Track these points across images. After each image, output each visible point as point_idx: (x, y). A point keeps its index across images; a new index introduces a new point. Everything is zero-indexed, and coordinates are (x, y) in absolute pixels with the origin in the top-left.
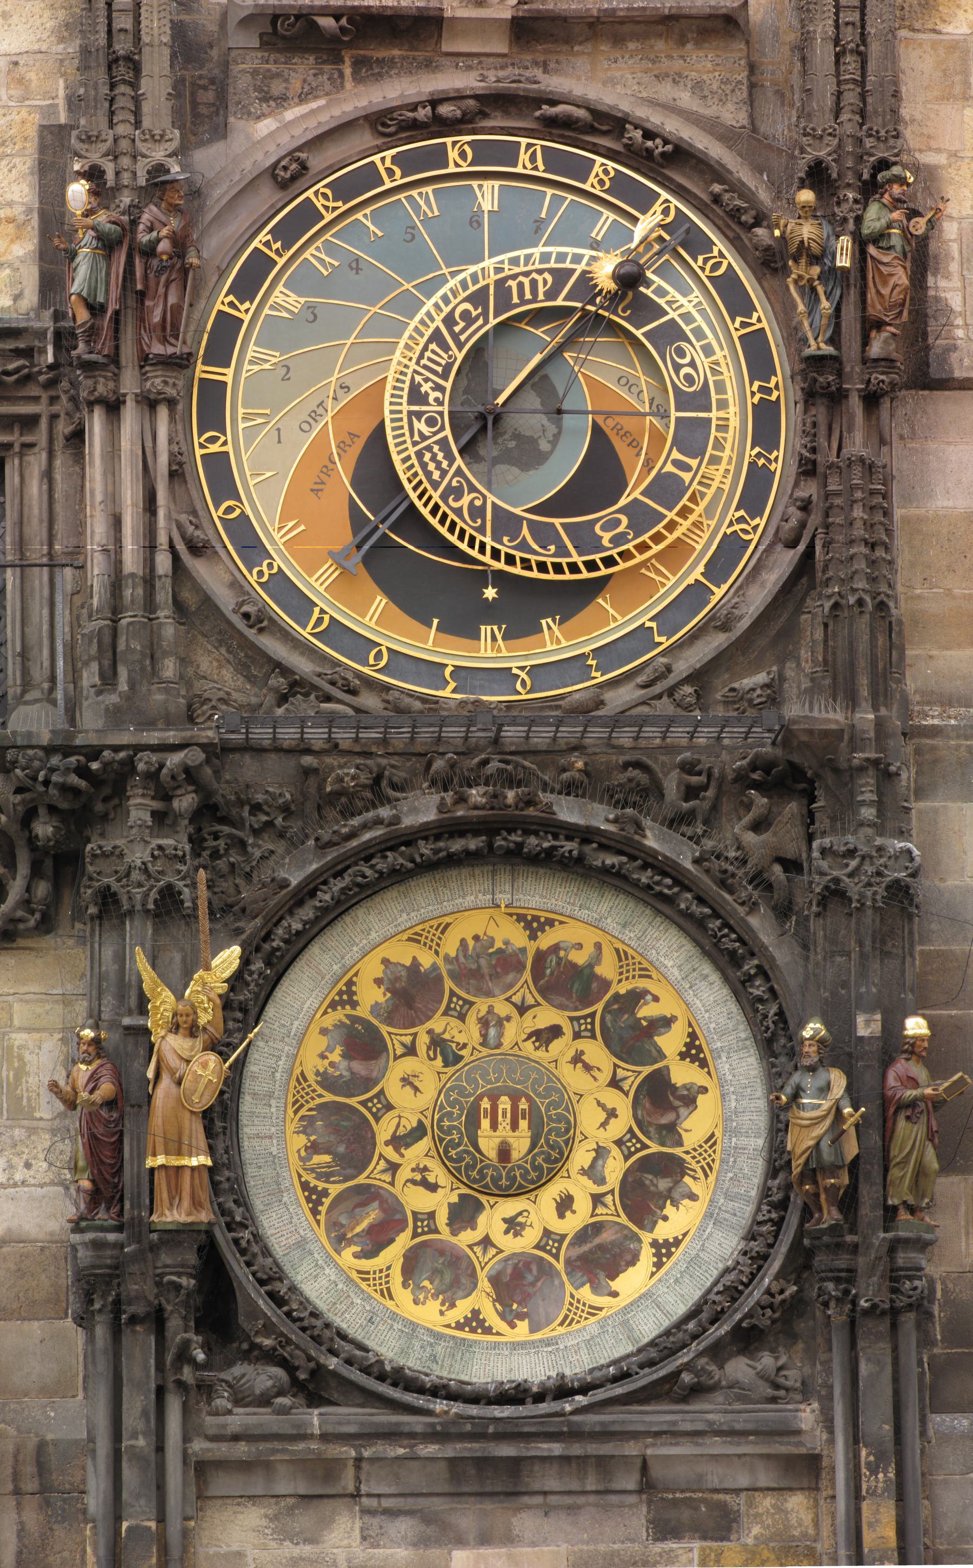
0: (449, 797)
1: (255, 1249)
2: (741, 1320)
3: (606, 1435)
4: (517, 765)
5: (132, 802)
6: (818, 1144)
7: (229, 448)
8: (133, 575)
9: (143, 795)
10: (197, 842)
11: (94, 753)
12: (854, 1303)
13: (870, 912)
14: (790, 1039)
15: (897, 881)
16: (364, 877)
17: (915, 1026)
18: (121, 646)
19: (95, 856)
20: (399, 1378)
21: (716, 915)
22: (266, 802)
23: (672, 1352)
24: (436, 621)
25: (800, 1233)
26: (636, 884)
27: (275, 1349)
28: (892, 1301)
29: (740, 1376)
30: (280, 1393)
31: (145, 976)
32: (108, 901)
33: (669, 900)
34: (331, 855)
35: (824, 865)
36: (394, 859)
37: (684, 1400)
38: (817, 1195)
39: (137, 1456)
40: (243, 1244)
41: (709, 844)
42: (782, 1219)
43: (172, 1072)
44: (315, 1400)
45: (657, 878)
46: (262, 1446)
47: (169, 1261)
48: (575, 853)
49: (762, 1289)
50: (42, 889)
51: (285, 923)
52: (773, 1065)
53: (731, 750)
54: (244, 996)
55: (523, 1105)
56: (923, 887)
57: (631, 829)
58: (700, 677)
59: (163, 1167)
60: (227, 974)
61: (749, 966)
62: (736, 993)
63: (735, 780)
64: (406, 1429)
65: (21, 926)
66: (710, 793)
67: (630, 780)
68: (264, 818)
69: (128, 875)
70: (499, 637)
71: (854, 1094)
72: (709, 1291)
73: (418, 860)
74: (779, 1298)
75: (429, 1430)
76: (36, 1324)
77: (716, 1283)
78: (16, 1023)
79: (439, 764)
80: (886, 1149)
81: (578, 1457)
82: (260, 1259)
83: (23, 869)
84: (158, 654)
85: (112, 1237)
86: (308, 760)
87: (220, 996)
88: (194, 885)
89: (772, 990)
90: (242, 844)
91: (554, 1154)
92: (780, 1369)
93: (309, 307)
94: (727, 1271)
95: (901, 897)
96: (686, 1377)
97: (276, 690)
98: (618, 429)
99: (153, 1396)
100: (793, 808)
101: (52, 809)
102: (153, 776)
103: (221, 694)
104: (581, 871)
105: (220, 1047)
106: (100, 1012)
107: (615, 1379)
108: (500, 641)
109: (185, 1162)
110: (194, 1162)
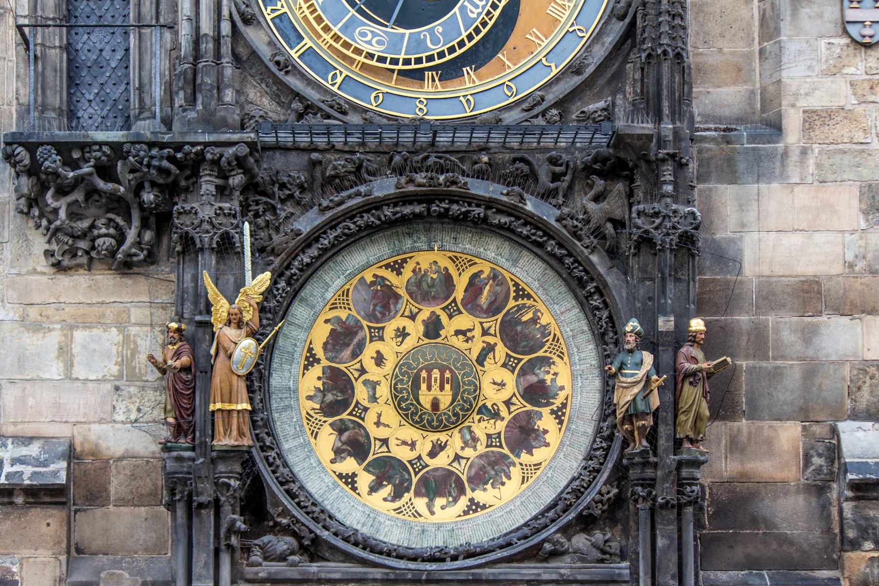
0: (403, 180)
1: (278, 462)
2: (582, 510)
4: (447, 159)
5: (203, 179)
10: (245, 208)
12: (654, 499)
14: (616, 333)
18: (199, 81)
19: (180, 213)
20: (366, 544)
21: (570, 255)
22: (289, 182)
23: (538, 531)
25: (621, 456)
26: (520, 235)
28: (678, 499)
29: (581, 545)
30: (293, 553)
31: (209, 290)
32: (188, 241)
33: (541, 245)
34: (329, 214)
35: (639, 222)
36: (370, 218)
37: (545, 560)
41: (566, 210)
42: (609, 447)
44: (314, 557)
45: (533, 231)
47: (223, 470)
48: (482, 215)
49: (596, 491)
50: (148, 236)
52: (605, 350)
53: (581, 150)
54: (273, 304)
55: (448, 375)
56: (702, 237)
57: (517, 199)
58: (562, 104)
59: (219, 410)
60: (263, 289)
61: (591, 287)
62: (581, 304)
63: (584, 169)
64: (371, 577)
65: (135, 259)
66: (568, 178)
67: (517, 169)
68: (288, 192)
69: (200, 226)
70: (437, 79)
73: (383, 219)
74: (606, 497)
75: (385, 577)
76: (143, 509)
78: (133, 320)
79: (397, 158)
80: (676, 403)
82: (281, 469)
83: (136, 223)
85: (187, 454)
86: (315, 156)
87: (257, 303)
88: (242, 233)
89: (605, 302)
90: (274, 208)
91: (467, 406)
92: (606, 542)
94: (574, 479)
95: (687, 243)
96: (548, 546)
97: (296, 111)
99: (212, 555)
100: (620, 186)
101: (153, 184)
103: (262, 113)
104: (485, 227)
106: (183, 313)
109: (233, 407)
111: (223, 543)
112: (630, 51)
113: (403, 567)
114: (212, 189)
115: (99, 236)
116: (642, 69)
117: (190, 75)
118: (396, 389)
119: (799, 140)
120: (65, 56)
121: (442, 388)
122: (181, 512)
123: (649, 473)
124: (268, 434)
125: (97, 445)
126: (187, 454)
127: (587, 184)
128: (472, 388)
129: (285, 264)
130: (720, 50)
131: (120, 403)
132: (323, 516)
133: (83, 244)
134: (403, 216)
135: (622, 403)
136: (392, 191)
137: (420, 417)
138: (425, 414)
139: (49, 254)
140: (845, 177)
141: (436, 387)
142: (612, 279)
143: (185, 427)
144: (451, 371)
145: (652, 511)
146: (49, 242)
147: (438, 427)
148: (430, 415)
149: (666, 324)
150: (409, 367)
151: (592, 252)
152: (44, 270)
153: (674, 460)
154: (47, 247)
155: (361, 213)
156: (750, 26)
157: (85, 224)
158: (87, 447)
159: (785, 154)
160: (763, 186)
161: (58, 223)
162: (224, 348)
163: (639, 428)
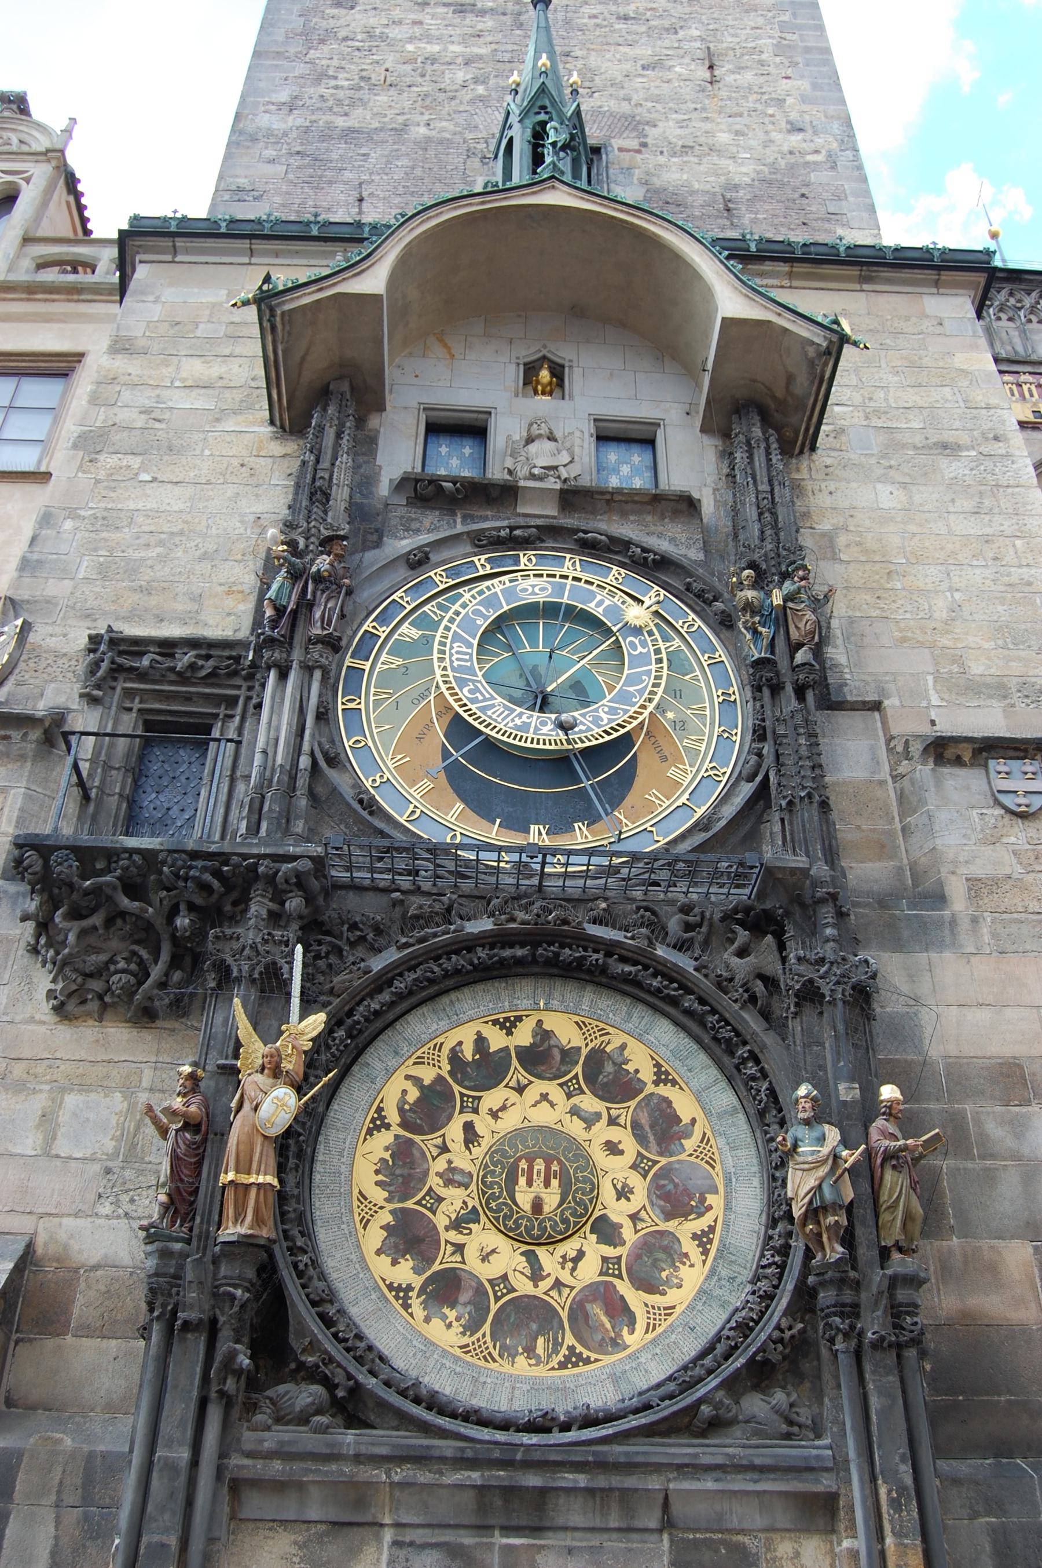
1: (311, 1271)
2: (755, 1354)
3: (630, 1467)
6: (820, 1186)
7: (362, 706)
9: (263, 896)
11: (223, 857)
13: (840, 1004)
14: (780, 1110)
16: (433, 972)
18: (266, 808)
19: (217, 937)
20: (433, 1403)
21: (714, 1011)
23: (688, 1386)
24: (498, 821)
30: (319, 1412)
37: (703, 1434)
39: (171, 1467)
40: (301, 1266)
42: (785, 1263)
44: (354, 1420)
46: (296, 1466)
47: (229, 1273)
48: (600, 961)
55: (555, 1167)
60: (315, 1033)
61: (742, 1051)
63: (723, 920)
64: (437, 1453)
66: (704, 929)
70: (544, 832)
71: (845, 1142)
72: (723, 1328)
74: (788, 1334)
75: (459, 1455)
76: (114, 1342)
77: (729, 1321)
81: (602, 1490)
83: (165, 956)
84: (293, 817)
85: (178, 1246)
89: (762, 1071)
90: (339, 951)
91: (580, 1210)
92: (792, 1405)
93: (423, 636)
94: (737, 1310)
95: (862, 997)
101: (192, 907)
104: (604, 980)
107: (636, 1411)
108: (544, 835)
110: (261, 1179)
111: (214, 1388)
112: (764, 811)
113: (487, 1438)
114: (264, 913)
115: (117, 972)
117: (257, 805)
118: (484, 1183)
119: (967, 908)
120: (124, 805)
121: (547, 1184)
125: (66, 1247)
128: (588, 1187)
129: (347, 1008)
130: (859, 827)
132: (370, 1357)
133: (96, 985)
134: (502, 962)
135: (802, 1193)
138: (522, 1217)
139: (51, 994)
140: (1028, 947)
141: (538, 1182)
145: (858, 1355)
147: (540, 1237)
148: (529, 1219)
149: (847, 1092)
150: (504, 1154)
152: (44, 1018)
154: (52, 986)
155: (449, 954)
157: (103, 958)
158: (52, 1249)
159: (953, 922)
160: (933, 955)
161: (66, 951)
163: (828, 1228)
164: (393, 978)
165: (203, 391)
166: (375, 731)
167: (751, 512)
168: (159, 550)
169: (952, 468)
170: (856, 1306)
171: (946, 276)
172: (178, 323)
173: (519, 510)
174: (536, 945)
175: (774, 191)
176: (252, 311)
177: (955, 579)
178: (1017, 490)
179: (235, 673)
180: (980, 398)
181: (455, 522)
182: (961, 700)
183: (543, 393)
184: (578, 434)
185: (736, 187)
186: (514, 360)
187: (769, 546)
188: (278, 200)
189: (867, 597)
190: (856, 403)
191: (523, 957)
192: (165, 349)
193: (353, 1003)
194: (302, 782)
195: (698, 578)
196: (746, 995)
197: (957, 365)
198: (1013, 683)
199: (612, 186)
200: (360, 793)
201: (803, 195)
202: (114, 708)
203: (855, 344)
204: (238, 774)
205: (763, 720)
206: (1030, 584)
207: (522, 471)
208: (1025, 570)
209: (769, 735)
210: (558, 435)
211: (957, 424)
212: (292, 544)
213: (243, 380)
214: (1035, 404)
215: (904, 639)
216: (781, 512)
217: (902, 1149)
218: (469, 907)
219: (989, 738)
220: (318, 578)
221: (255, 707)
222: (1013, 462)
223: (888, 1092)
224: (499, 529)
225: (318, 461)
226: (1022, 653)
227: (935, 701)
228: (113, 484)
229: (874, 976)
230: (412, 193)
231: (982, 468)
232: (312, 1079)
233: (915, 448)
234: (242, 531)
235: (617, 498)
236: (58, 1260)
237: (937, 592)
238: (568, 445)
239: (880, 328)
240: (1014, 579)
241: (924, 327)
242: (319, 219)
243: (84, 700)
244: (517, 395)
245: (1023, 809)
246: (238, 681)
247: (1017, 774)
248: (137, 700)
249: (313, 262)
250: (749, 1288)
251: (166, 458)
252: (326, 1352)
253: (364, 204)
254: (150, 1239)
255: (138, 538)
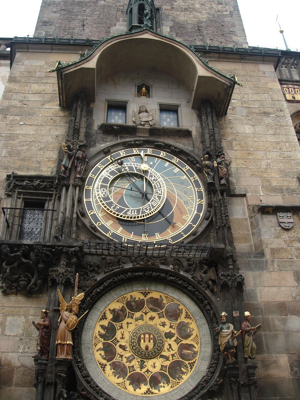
2: (209, 389)
8: (67, 217)
14: (216, 319)
15: (239, 282)
16: (115, 280)
17: (247, 313)
18: (64, 230)
21: (197, 291)
24: (133, 233)
26: (178, 284)
27: (86, 395)
33: (186, 288)
35: (222, 278)
38: (228, 355)
40: (80, 367)
42: (218, 363)
43: (64, 320)
51: (96, 290)
52: (213, 325)
55: (152, 336)
57: (177, 270)
61: (206, 302)
63: (199, 263)
65: (34, 290)
66: (194, 266)
67: (176, 262)
68: (92, 268)
69: (59, 275)
74: (219, 382)
76: (26, 388)
77: (202, 380)
78: (30, 314)
79: (133, 258)
80: (243, 344)
82: (84, 371)
84: (72, 233)
85: (45, 362)
89: (211, 308)
90: (87, 273)
91: (159, 349)
94: (204, 376)
95: (240, 285)
98: (171, 199)
101: (43, 262)
102: (67, 253)
105: (78, 315)
108: (146, 237)
110: (68, 343)
112: (211, 229)
114: (65, 263)
116: (217, 232)
117: (61, 229)
118: (131, 342)
119: (270, 258)
120: (20, 228)
121: (149, 341)
122: (40, 387)
123: (235, 372)
124: (80, 357)
125: (10, 361)
126: (45, 362)
127: (201, 268)
131: (21, 345)
133: (15, 285)
134: (136, 276)
135: (223, 343)
136: (131, 266)
137: (141, 353)
138: (143, 351)
140: (288, 269)
141: (147, 341)
142: (213, 298)
143: (45, 351)
144: (153, 335)
145: (238, 388)
146: (2, 283)
148: (145, 352)
150: (137, 333)
151: (206, 289)
153: (245, 366)
154: (2, 285)
156: (247, 226)
157: (16, 276)
159: (266, 262)
161: (6, 275)
162: (64, 319)
163: (231, 353)
164: (104, 282)
165: (38, 95)
166: (95, 205)
167: (207, 136)
168: (27, 147)
169: (267, 120)
170: (238, 374)
171: (266, 58)
172: (30, 72)
173: (137, 135)
174: (145, 272)
175: (213, 24)
176: (55, 74)
177: (268, 156)
178: (287, 127)
179: (51, 187)
180: (276, 98)
181: (118, 139)
182: (269, 193)
183: (143, 96)
184: (155, 110)
185: (202, 22)
186: (134, 85)
187: (212, 147)
188: (57, 25)
189: (242, 161)
190: (239, 99)
191: (142, 275)
192: (26, 81)
193: (92, 290)
194: (74, 222)
195: (192, 157)
196: (206, 286)
197: (269, 87)
198: (284, 188)
199: (163, 21)
200: (91, 225)
201: (222, 25)
202: (15, 198)
203: (239, 84)
204: (54, 218)
205: (211, 201)
206: (290, 157)
207: (138, 123)
208: (289, 153)
209: (213, 207)
210: (148, 110)
211: (269, 106)
212: (69, 147)
213: (51, 91)
214: (293, 94)
215: (253, 175)
216: (216, 136)
217: (250, 330)
218: (125, 259)
219: (277, 206)
220: (78, 159)
221: (58, 197)
222: (286, 118)
223: (247, 313)
224: (131, 141)
225: (75, 119)
226: (287, 179)
227: (262, 194)
228: (12, 125)
229: (243, 279)
230: (100, 24)
231: (276, 120)
232: (81, 312)
233: (257, 113)
234: (52, 141)
235: (167, 131)
236: (8, 365)
237: (263, 160)
238: (151, 113)
239: (246, 74)
240: (285, 156)
241: (259, 74)
242: (73, 38)
243: (6, 196)
244: (135, 97)
245: (287, 228)
246: (53, 189)
247: (285, 217)
248: (22, 195)
249: (71, 52)
250: (208, 370)
251: (28, 117)
252: (88, 391)
253: (85, 27)
254: (35, 360)
255: (20, 143)
